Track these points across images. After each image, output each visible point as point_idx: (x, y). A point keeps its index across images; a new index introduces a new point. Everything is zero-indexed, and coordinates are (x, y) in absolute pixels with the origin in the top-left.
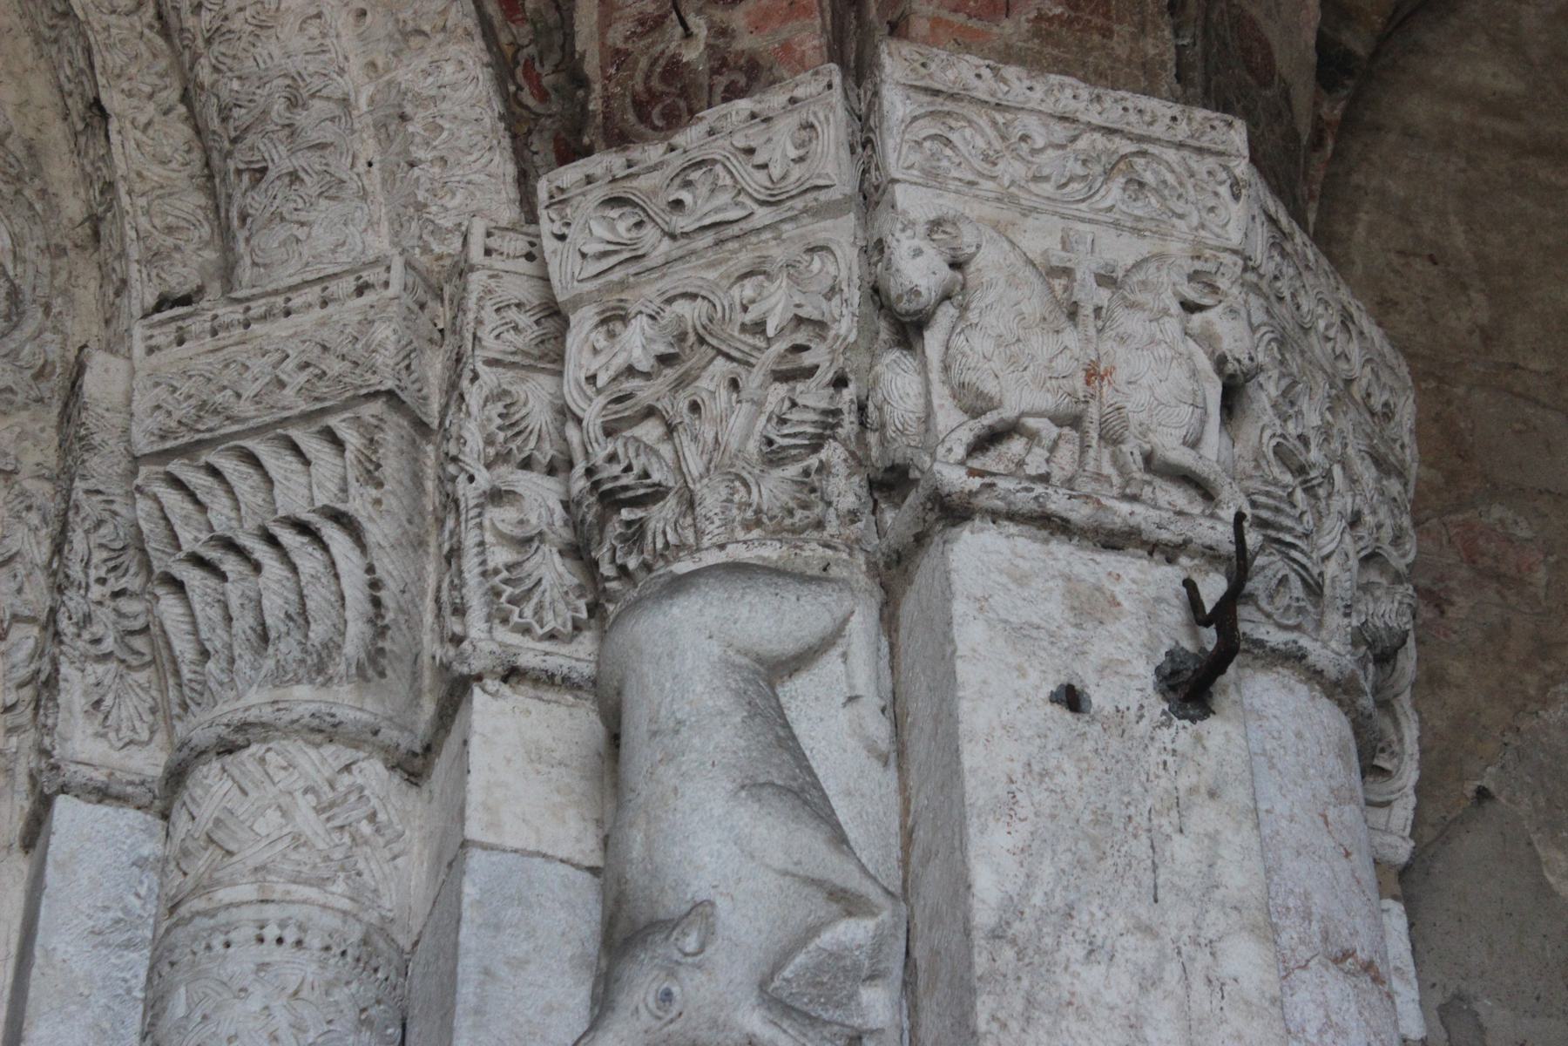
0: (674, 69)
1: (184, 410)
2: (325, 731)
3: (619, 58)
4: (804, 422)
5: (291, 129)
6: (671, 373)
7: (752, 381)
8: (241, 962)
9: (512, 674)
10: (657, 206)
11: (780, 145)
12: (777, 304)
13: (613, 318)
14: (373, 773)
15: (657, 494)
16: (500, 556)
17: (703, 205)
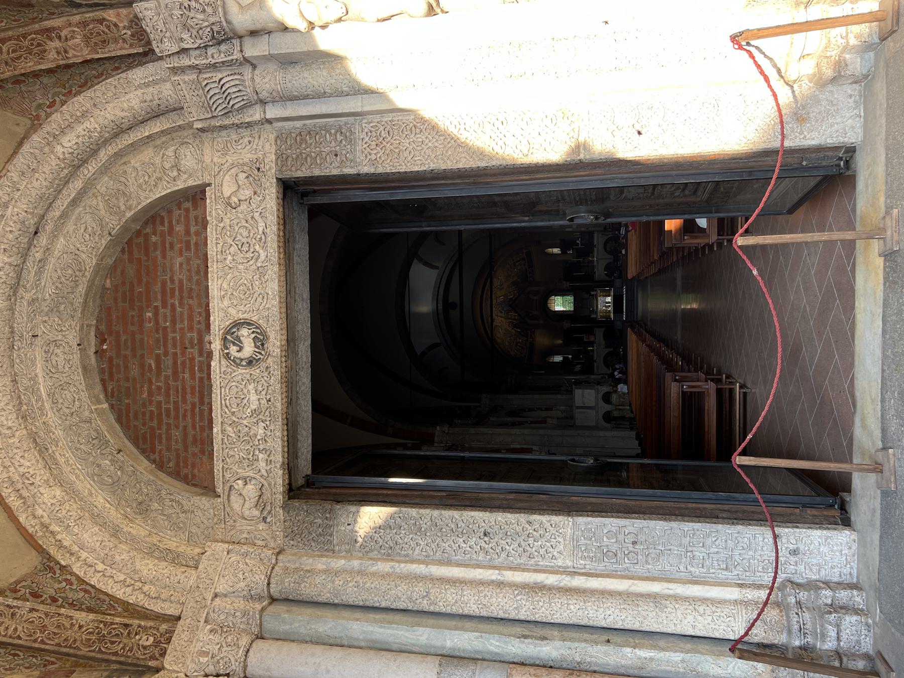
0: (133, 35)
1: (204, 109)
2: (253, 79)
3: (131, 45)
4: (198, 6)
5: (151, 101)
6: (191, 29)
7: (192, 15)
8: (289, 85)
9: (241, 51)
10: (162, 35)
11: (149, 14)
12: (177, 12)
13: (182, 40)
14: (257, 72)
15: (212, 29)
16: (222, 55)
17: (161, 26)
